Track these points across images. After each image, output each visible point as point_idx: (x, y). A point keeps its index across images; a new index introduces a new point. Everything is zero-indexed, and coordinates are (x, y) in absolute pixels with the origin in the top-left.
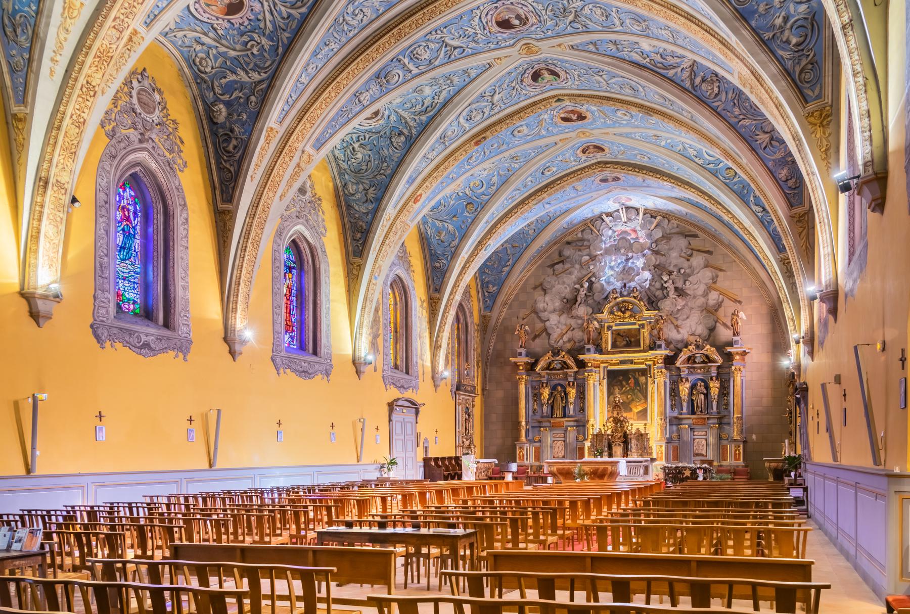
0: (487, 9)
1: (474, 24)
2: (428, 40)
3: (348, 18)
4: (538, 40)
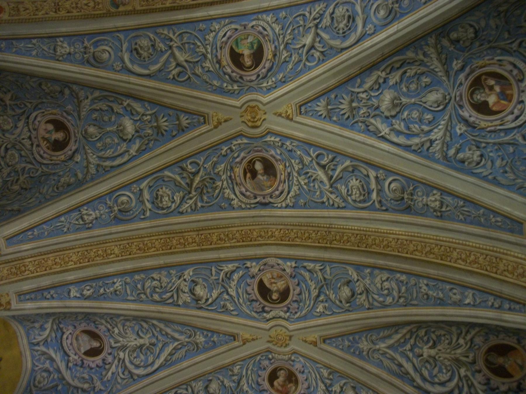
2: (345, 201)
3: (395, 294)
4: (241, 135)
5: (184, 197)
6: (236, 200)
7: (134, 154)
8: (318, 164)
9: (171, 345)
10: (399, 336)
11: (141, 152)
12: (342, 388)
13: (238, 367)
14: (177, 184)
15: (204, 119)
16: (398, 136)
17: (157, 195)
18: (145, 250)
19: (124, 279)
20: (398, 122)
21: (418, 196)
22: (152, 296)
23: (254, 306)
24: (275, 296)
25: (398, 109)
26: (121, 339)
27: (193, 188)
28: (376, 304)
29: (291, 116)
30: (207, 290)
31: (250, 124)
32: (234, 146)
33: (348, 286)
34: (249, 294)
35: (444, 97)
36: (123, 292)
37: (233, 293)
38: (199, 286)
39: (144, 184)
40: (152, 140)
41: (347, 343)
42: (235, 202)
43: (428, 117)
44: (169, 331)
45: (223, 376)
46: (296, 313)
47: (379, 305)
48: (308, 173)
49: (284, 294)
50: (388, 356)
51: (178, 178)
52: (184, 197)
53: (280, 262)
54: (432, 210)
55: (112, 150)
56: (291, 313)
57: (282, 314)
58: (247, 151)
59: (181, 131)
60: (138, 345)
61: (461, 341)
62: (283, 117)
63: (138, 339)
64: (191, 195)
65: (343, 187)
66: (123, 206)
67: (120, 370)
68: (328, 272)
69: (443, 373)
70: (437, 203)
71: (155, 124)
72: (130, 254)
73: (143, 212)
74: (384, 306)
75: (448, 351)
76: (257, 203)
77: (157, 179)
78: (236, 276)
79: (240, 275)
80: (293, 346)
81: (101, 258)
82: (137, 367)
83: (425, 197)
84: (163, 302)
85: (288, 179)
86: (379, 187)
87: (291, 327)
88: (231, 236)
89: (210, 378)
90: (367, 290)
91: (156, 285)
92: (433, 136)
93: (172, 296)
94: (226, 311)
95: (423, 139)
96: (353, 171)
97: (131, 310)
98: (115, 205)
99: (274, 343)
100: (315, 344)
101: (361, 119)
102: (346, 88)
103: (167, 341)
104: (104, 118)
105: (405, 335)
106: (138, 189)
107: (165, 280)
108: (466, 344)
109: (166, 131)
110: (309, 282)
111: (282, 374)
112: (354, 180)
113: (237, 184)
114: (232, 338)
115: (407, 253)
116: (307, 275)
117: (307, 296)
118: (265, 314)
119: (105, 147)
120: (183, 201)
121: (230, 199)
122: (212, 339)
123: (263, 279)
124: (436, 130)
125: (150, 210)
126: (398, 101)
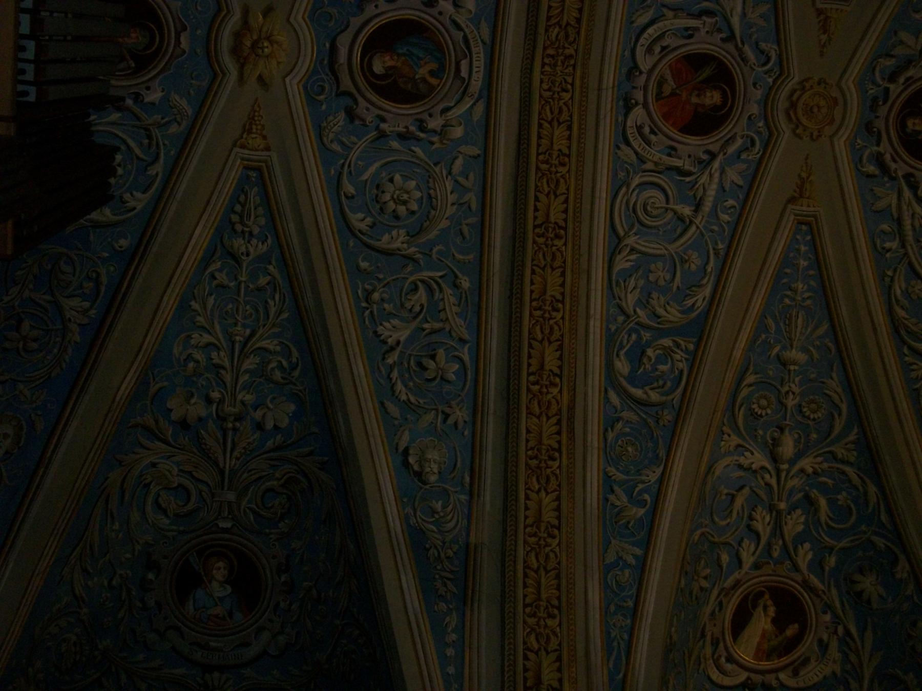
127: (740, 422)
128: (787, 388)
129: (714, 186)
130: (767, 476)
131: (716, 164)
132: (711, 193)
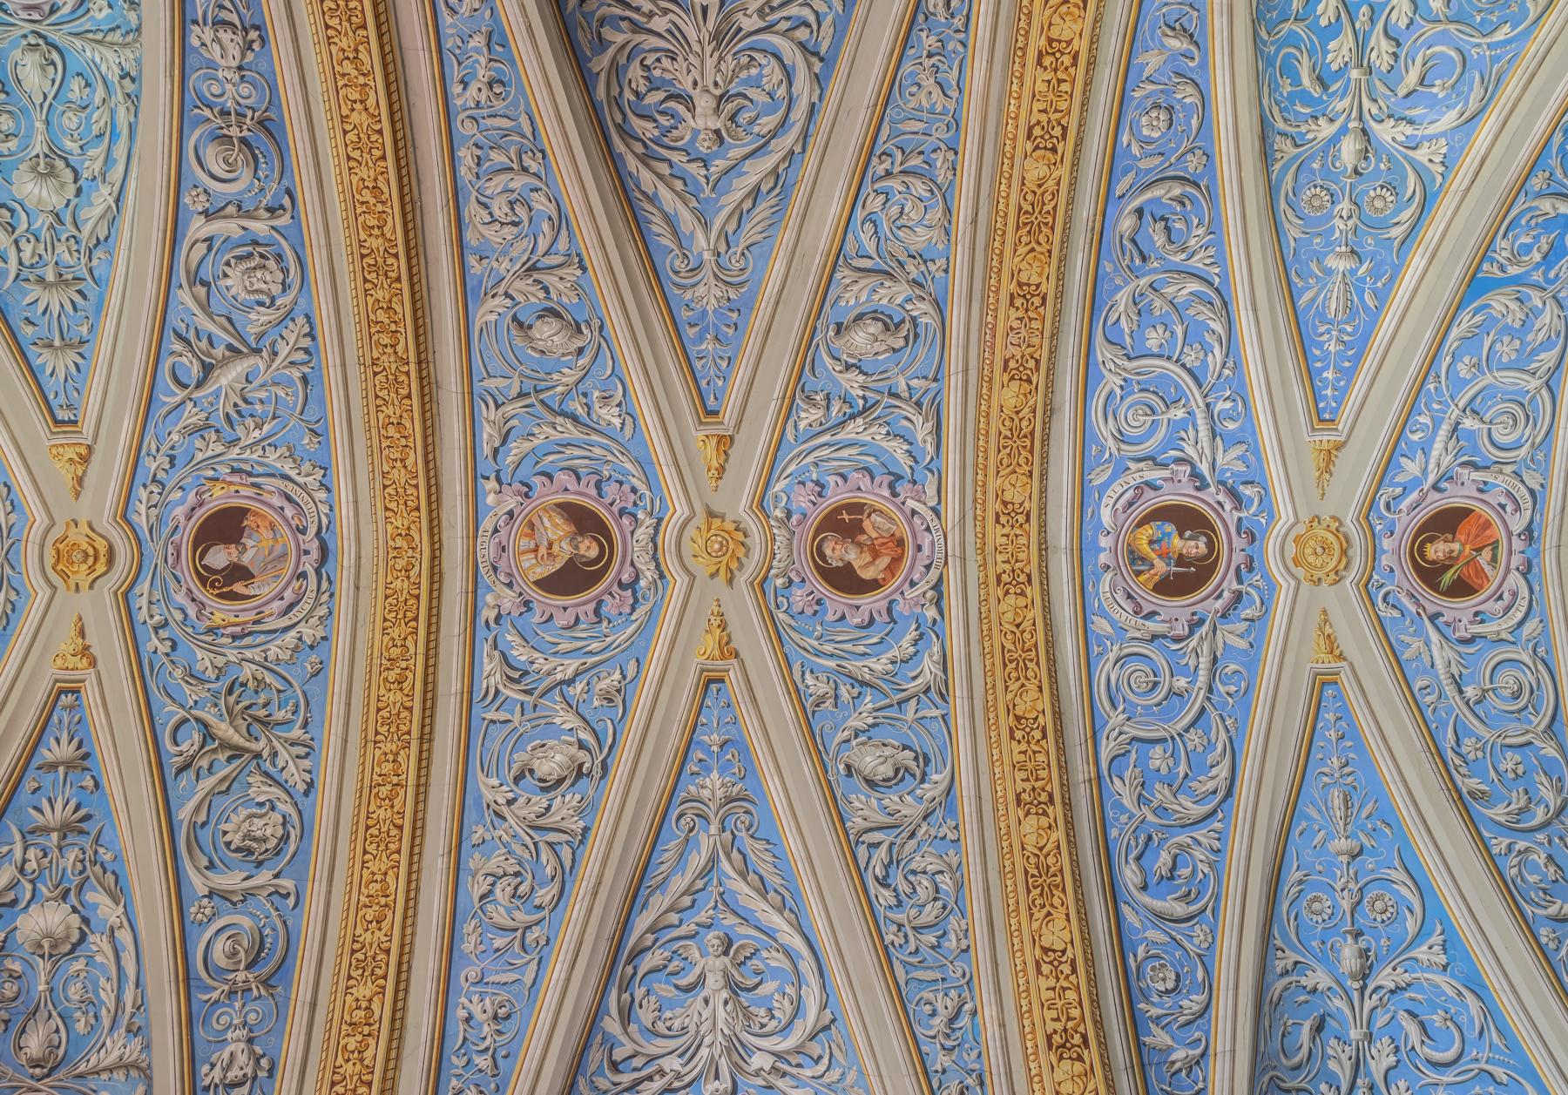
0: (309, 508)
1: (272, 457)
2: (289, 315)
3: (519, 182)
5: (266, 774)
6: (301, 627)
7: (121, 910)
8: (199, 385)
9: (729, 884)
10: (665, 194)
11: (118, 893)
12: (848, 367)
13: (809, 680)
14: (224, 788)
15: (66, 692)
16: (115, 161)
17: (238, 850)
18: (386, 905)
19: (465, 986)
20: (87, 164)
21: (222, 95)
22: (540, 907)
23: (614, 612)
24: (589, 549)
25: (60, 164)
26: (704, 1052)
27: (247, 744)
28: (562, 244)
29: (83, 451)
30: (551, 743)
31: (101, 568)
32: (152, 617)
33: (530, 327)
34: (577, 619)
35: (33, 47)
36: (504, 995)
37: (572, 665)
38: (536, 764)
39: (197, 883)
40: (96, 852)
41: (708, 346)
42: (308, 632)
43: (76, 89)
44: (679, 883)
45: (835, 728)
46: (634, 490)
47: (564, 232)
48: (227, 415)
49: (582, 520)
50: (730, 228)
51: (208, 783)
52: (266, 774)
53: (487, 524)
54: (250, 56)
55: (102, 981)
56: (635, 504)
57: (643, 533)
58: (172, 584)
59: (86, 763)
60: (725, 994)
61: (659, 24)
62: (84, 472)
63: (704, 993)
64: (265, 754)
65: (253, 316)
66: (242, 954)
67: (809, 1073)
68: (501, 383)
69: (761, 76)
70: (226, 36)
71: (55, 836)
72: (388, 952)
73: (275, 898)
74: (561, 220)
75: (692, 59)
76: (318, 572)
77: (194, 842)
78: (520, 654)
79: (518, 640)
80: (741, 509)
81: (372, 1041)
82: (798, 1009)
83: (220, 74)
84: (564, 877)
85: (250, 474)
86: (231, 209)
87: (681, 510)
88: (395, 652)
89: (841, 767)
90: (528, 270)
91: (508, 889)
92: (113, 75)
93: (550, 844)
94: (619, 697)
95: (120, 97)
96: (205, 284)
97: (568, 979)
98: (231, 977)
99: (734, 565)
100: (725, 443)
101: (83, 261)
102: (7, 292)
103: (715, 896)
104: (9, 994)
105: (660, 176)
106: (206, 900)
107: (496, 862)
108: (666, 11)
109: (78, 808)
110: (536, 441)
111: (838, 552)
112: (229, 282)
113: (256, 622)
114: (714, 687)
115: (380, 132)
116: (516, 448)
117: (577, 452)
118: (643, 583)
119: (90, 1003)
120: (276, 776)
121: (297, 646)
122: (715, 748)
123: (538, 577)
124: (103, 69)
125: (276, 876)
126: (42, 161)
127: (1412, 178)
128: (1350, 223)
129: (1435, 453)
130: (1375, 111)
131: (1431, 478)
132: (1438, 446)
